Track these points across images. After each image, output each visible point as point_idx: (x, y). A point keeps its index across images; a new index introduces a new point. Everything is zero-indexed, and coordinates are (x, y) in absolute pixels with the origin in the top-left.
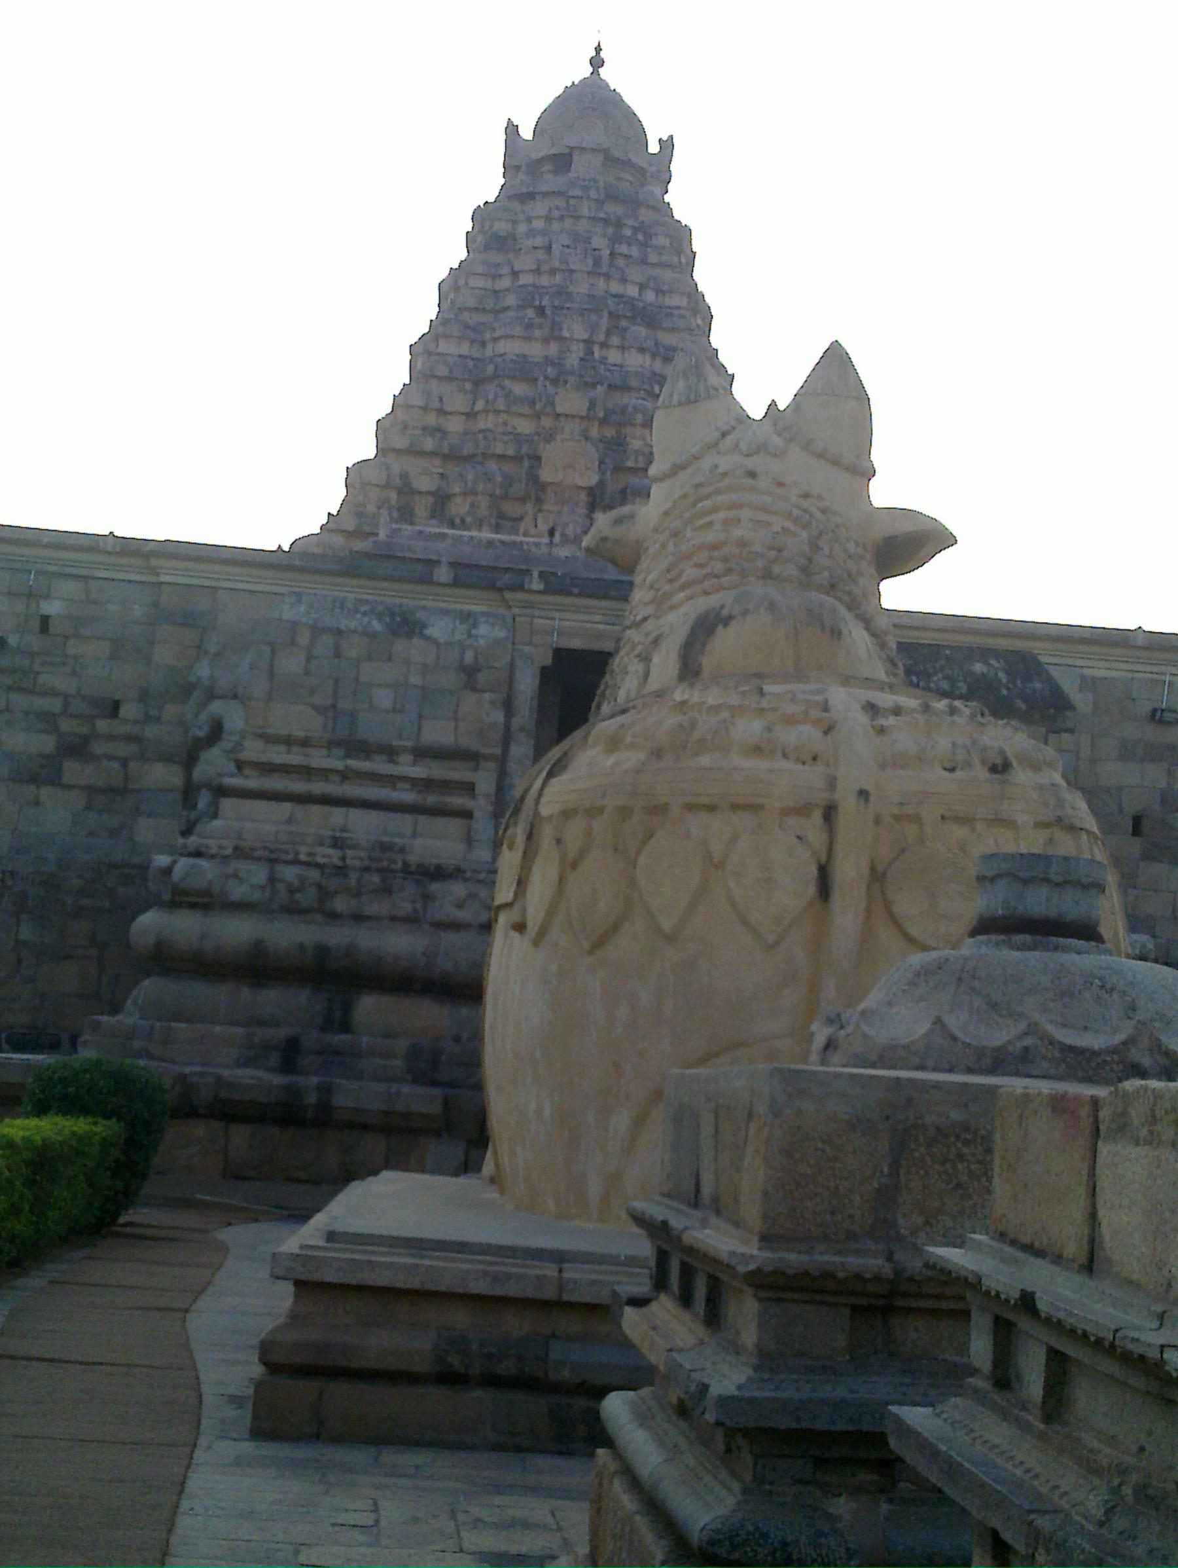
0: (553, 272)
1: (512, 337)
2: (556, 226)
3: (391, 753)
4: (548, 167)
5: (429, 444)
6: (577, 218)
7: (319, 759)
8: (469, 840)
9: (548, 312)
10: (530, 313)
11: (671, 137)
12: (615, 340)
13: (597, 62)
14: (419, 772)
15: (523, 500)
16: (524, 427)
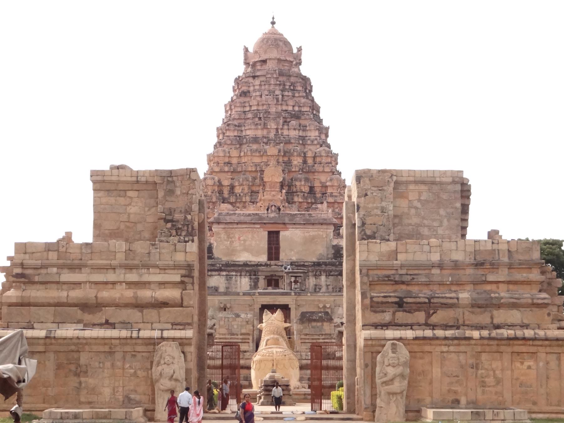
0: (263, 105)
1: (251, 129)
2: (263, 87)
3: (237, 335)
4: (258, 64)
5: (226, 169)
6: (270, 84)
7: (227, 337)
8: (249, 346)
9: (262, 119)
10: (257, 119)
11: (301, 47)
12: (286, 127)
13: (273, 23)
14: (241, 337)
15: (259, 186)
16: (257, 160)
